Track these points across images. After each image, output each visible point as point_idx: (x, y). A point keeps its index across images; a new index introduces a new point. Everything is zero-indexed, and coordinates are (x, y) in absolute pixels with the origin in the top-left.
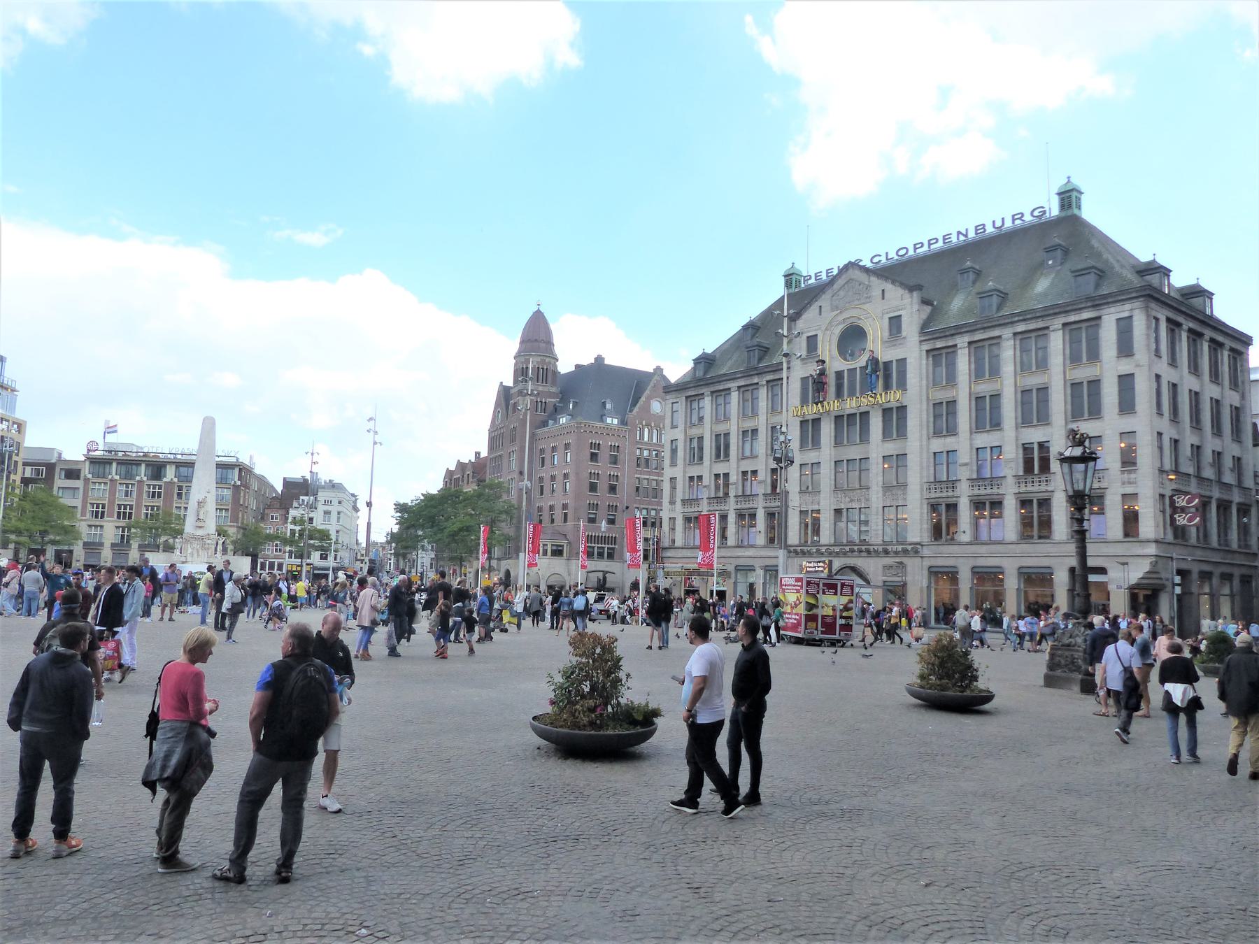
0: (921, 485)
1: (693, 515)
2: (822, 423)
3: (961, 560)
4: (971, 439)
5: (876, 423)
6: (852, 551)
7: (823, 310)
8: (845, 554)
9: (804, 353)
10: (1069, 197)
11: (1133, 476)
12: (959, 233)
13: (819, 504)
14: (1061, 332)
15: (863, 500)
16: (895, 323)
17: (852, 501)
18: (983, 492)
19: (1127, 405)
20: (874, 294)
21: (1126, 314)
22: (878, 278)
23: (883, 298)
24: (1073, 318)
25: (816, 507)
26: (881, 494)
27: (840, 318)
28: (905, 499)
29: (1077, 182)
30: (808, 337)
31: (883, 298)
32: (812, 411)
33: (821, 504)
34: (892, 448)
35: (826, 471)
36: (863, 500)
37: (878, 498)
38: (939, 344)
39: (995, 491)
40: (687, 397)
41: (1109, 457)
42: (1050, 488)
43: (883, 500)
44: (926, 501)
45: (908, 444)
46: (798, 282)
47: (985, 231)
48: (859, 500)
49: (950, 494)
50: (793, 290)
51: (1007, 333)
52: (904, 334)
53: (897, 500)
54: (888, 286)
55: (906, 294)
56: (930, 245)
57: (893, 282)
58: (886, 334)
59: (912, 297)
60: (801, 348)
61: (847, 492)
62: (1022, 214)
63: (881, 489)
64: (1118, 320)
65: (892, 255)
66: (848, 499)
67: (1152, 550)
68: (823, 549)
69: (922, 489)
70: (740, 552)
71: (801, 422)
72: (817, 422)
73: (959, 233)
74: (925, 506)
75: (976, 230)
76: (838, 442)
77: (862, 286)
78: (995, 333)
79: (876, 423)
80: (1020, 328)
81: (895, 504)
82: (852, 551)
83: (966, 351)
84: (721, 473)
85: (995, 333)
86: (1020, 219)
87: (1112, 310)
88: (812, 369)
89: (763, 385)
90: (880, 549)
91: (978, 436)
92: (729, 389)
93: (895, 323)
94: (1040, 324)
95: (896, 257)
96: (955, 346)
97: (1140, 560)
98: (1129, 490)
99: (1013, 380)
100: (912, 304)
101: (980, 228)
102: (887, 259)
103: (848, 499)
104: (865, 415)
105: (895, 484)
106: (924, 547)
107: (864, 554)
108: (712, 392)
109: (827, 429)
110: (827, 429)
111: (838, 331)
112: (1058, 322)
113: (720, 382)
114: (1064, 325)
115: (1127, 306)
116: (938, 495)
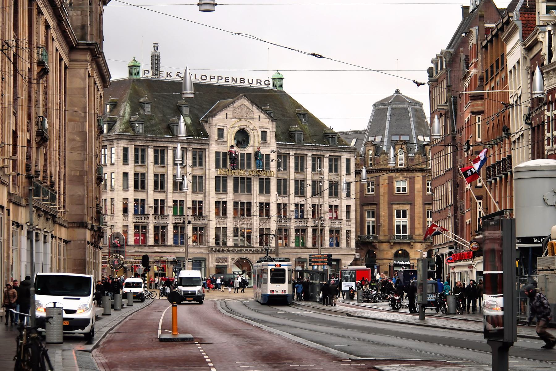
1: (140, 225)
2: (228, 180)
3: (291, 256)
4: (294, 199)
5: (255, 186)
6: (250, 250)
7: (228, 116)
8: (241, 252)
9: (217, 137)
10: (279, 81)
11: (350, 223)
12: (233, 78)
13: (227, 224)
14: (328, 159)
15: (249, 224)
16: (264, 135)
17: (243, 224)
18: (301, 225)
19: (348, 195)
20: (254, 116)
21: (349, 158)
22: (257, 109)
23: (259, 120)
24: (332, 154)
25: (225, 226)
26: (258, 222)
27: (240, 124)
28: (270, 225)
29: (283, 74)
30: (218, 129)
31: (259, 120)
32: (223, 172)
33: (228, 224)
34: (263, 199)
35: (230, 207)
38: (283, 151)
39: (305, 225)
40: (135, 145)
41: (343, 215)
42: (325, 225)
45: (271, 198)
46: (137, 73)
47: (245, 82)
49: (288, 224)
50: (138, 77)
51: (310, 154)
52: (268, 142)
53: (266, 225)
54: (262, 115)
55: (271, 122)
56: (218, 79)
57: (264, 114)
58: (260, 139)
59: (273, 124)
60: (214, 135)
62: (261, 81)
64: (346, 159)
65: (198, 77)
67: (354, 252)
68: (231, 249)
70: (176, 250)
71: (216, 177)
72: (225, 179)
73: (233, 78)
75: (241, 80)
76: (236, 190)
77: (248, 110)
78: (305, 152)
79: (255, 186)
80: (315, 153)
81: (265, 227)
82: (250, 250)
83: (293, 157)
84: (159, 199)
85: (305, 152)
86: (260, 83)
87: (345, 154)
88: (224, 149)
89: (190, 150)
91: (296, 198)
92: (167, 147)
93: (264, 135)
94: (321, 153)
95: (200, 80)
96: (289, 154)
97: (351, 256)
98: (349, 229)
99: (311, 176)
100: (273, 128)
101: (243, 81)
102: (196, 79)
103: (241, 223)
104: (249, 180)
108: (154, 146)
109: (230, 185)
110: (230, 185)
111: (236, 130)
112: (327, 154)
113: (161, 141)
114: (329, 156)
115: (349, 155)
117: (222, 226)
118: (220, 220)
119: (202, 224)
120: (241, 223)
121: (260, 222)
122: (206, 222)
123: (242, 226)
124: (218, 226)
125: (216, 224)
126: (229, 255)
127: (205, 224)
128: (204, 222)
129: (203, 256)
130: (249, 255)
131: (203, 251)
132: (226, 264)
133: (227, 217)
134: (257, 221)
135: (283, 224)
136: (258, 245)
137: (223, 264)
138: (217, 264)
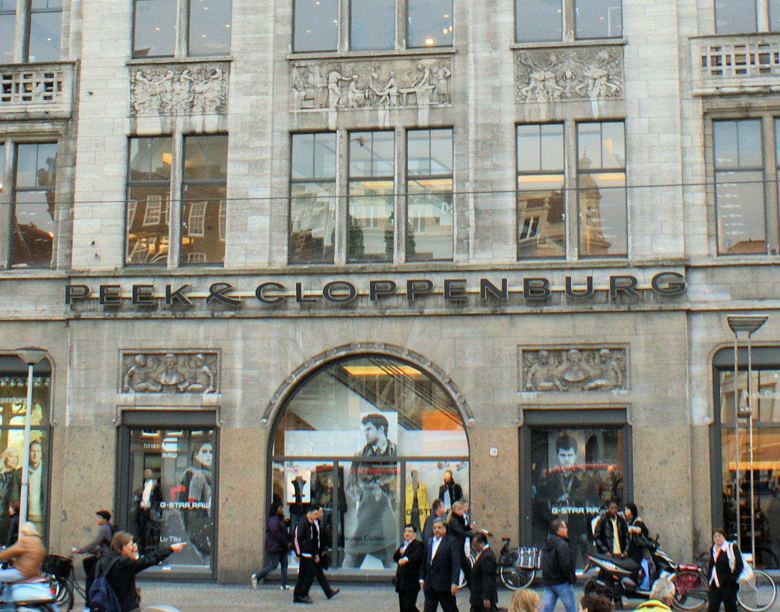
0: (684, 44)
13: (221, 110)
15: (424, 102)
17: (372, 99)
25: (212, 123)
26: (508, 76)
28: (617, 96)
33: (238, 105)
36: (424, 102)
37: (496, 92)
43: (521, 100)
44: (695, 109)
48: (407, 98)
61: (348, 67)
63: (509, 57)
66: (354, 94)
68: (245, 289)
69: (683, 63)
74: (695, 124)
81: (570, 112)
90: (516, 286)
105: (568, 40)
106: (697, 277)
107: (431, 306)
116: (753, 82)
117: (180, 128)
118: (163, 82)
119: (27, 119)
120: (354, 94)
121: (524, 77)
122: (61, 105)
123: (365, 119)
124: (150, 125)
125: (134, 113)
126: (238, 328)
127: (45, 118)
128: (36, 107)
129: (34, 337)
130: (417, 326)
131: (28, 311)
132: (209, 399)
133: (227, 71)
134: (494, 70)
135: (761, 81)
136: (507, 254)
137: (186, 401)
138: (130, 399)
